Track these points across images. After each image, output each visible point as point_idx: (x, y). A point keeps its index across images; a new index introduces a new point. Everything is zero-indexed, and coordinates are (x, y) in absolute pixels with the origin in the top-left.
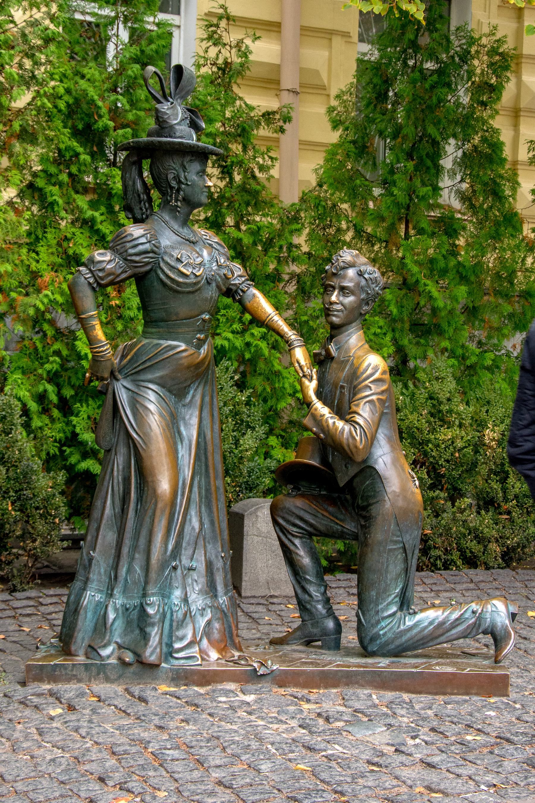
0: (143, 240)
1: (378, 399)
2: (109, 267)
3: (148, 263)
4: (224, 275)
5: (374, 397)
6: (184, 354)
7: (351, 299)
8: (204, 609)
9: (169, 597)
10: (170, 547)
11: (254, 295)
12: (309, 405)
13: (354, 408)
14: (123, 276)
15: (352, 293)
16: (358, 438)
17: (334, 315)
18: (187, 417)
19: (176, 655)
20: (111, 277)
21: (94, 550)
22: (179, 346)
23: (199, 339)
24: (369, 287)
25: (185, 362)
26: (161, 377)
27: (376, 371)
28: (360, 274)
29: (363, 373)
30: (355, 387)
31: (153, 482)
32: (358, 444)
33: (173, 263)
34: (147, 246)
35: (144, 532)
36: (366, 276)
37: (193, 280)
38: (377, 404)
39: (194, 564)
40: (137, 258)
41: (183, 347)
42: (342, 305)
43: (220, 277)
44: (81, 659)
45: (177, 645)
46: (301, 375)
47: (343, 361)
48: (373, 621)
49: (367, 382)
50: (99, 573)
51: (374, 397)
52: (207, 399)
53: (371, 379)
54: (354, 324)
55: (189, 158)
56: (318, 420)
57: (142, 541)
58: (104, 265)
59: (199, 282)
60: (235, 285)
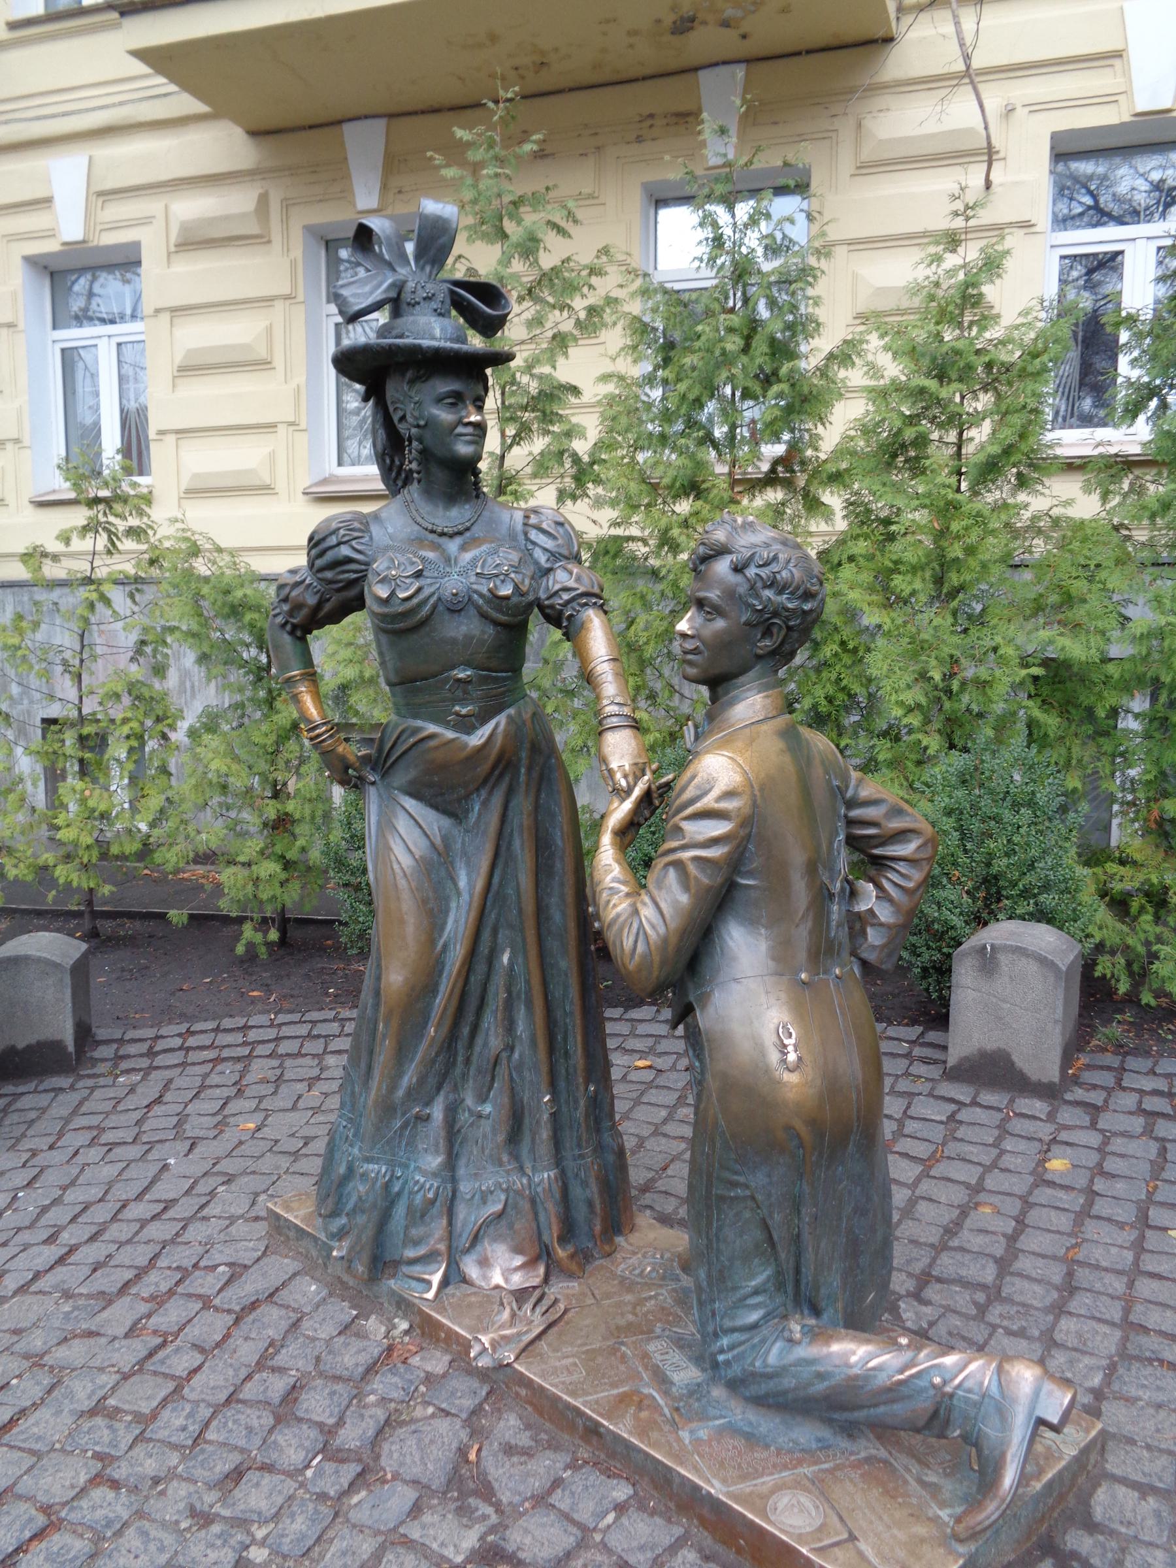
0: (333, 540)
1: (696, 859)
2: (294, 594)
4: (490, 590)
5: (687, 855)
6: (433, 743)
7: (720, 624)
9: (405, 1166)
11: (582, 626)
14: (327, 607)
20: (304, 612)
22: (418, 730)
23: (457, 714)
24: (758, 596)
27: (706, 793)
28: (738, 569)
34: (345, 551)
41: (432, 728)
43: (481, 595)
45: (410, 1253)
54: (742, 679)
60: (552, 607)
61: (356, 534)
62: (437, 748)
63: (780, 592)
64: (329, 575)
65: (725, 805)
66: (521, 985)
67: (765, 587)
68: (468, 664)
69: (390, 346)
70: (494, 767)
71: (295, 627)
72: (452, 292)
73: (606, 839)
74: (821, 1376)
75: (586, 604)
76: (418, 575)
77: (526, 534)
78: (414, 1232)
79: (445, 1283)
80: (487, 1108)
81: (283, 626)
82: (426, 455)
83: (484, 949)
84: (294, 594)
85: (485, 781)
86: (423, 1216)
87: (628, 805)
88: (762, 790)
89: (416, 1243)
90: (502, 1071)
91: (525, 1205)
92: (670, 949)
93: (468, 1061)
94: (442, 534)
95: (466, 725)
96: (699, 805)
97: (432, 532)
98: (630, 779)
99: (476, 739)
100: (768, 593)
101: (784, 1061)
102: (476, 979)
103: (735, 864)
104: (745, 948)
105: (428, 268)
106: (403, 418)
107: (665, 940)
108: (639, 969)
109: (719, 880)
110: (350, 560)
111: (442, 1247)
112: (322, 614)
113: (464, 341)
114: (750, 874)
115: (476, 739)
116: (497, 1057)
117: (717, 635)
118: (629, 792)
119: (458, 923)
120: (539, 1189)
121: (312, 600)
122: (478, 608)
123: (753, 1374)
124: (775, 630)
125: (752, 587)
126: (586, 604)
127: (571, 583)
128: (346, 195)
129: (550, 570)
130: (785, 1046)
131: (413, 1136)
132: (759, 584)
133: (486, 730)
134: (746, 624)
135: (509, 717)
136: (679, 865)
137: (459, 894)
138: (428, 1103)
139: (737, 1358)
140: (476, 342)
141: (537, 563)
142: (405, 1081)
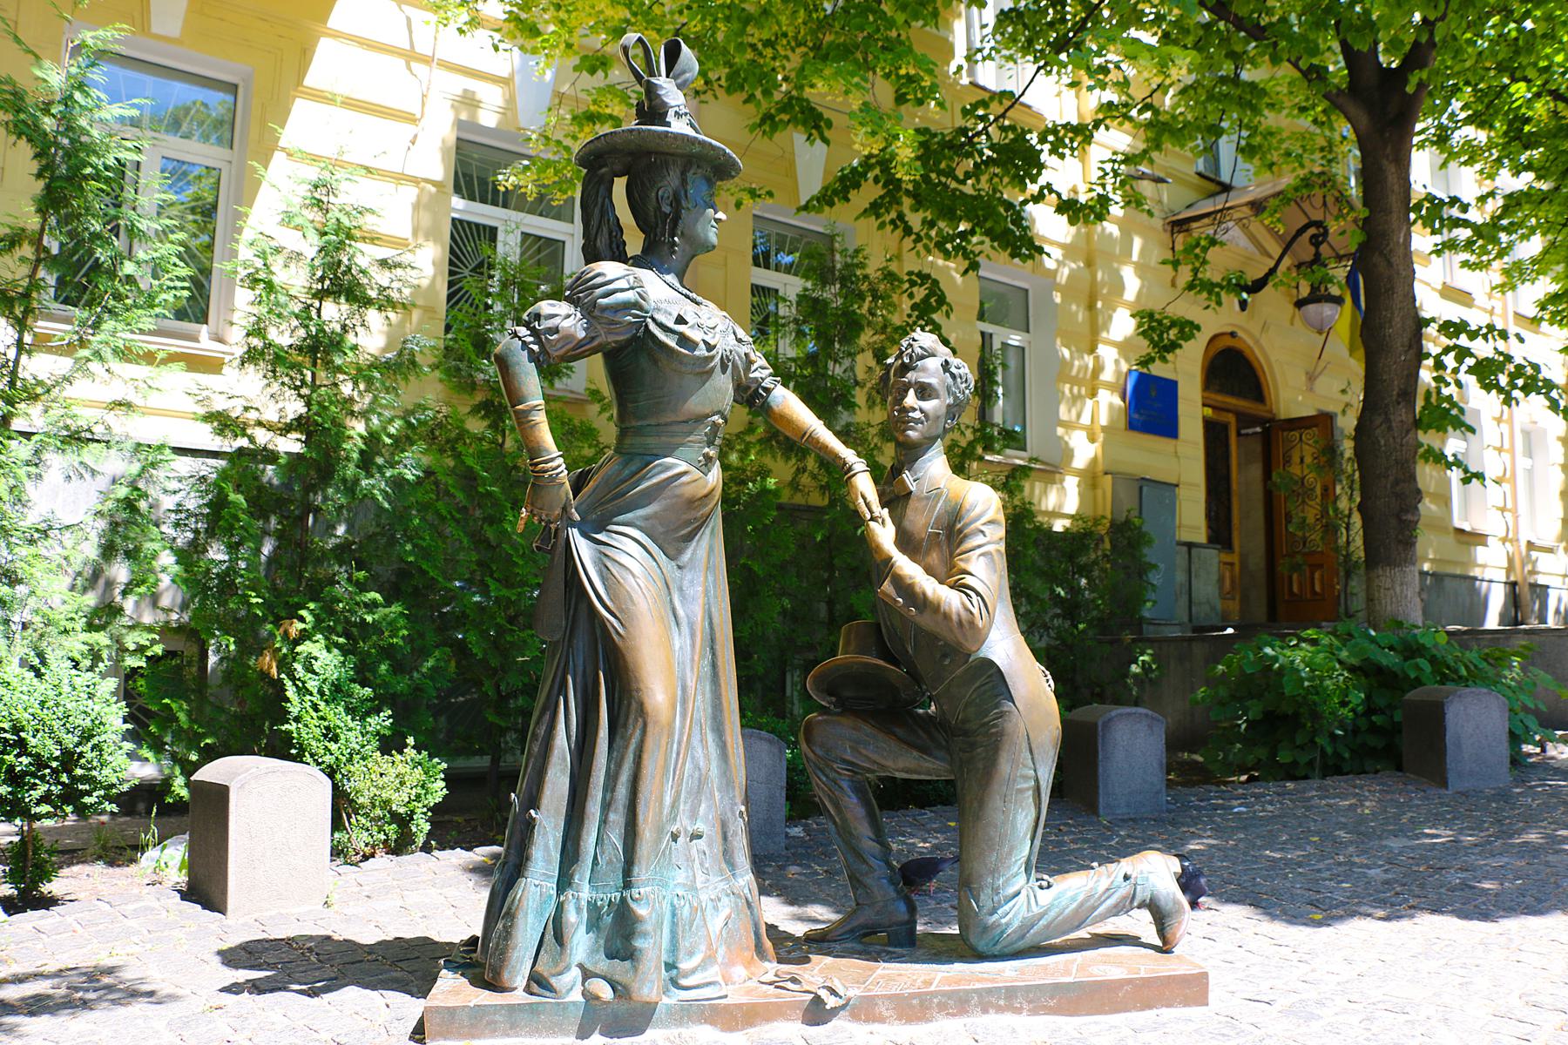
6: (684, 479)
10: (668, 800)
12: (888, 561)
13: (962, 565)
16: (975, 611)
17: (912, 429)
18: (686, 583)
19: (684, 982)
21: (536, 807)
26: (647, 518)
30: (960, 531)
31: (638, 690)
33: (671, 324)
35: (624, 777)
36: (953, 370)
37: (702, 351)
38: (996, 557)
39: (701, 826)
42: (922, 411)
44: (519, 996)
46: (868, 516)
47: (928, 498)
48: (989, 904)
49: (978, 524)
50: (546, 847)
51: (990, 548)
53: (984, 520)
56: (906, 589)
57: (622, 791)
58: (556, 321)
59: (713, 357)
74: (1073, 899)
89: (691, 954)
110: (636, 305)
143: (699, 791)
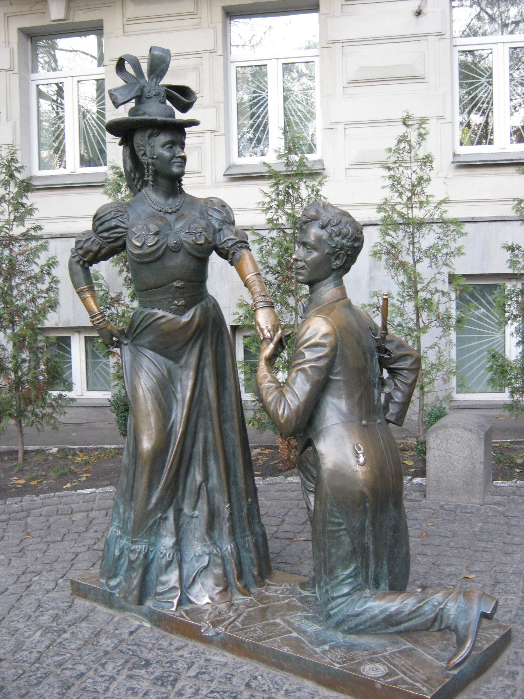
0: (108, 217)
1: (311, 367)
2: (85, 246)
3: (117, 239)
4: (193, 241)
5: (306, 366)
6: (163, 320)
7: (315, 254)
8: (201, 556)
10: (154, 500)
14: (103, 251)
15: (315, 248)
16: (280, 412)
18: (184, 377)
20: (91, 254)
22: (155, 314)
24: (333, 240)
25: (165, 327)
26: (150, 342)
27: (315, 335)
29: (301, 338)
32: (280, 417)
40: (105, 234)
42: (305, 262)
46: (262, 338)
51: (306, 366)
52: (209, 359)
54: (326, 281)
55: (148, 132)
60: (223, 249)
61: (120, 214)
62: (164, 323)
63: (343, 238)
64: (105, 234)
65: (322, 341)
66: (210, 447)
67: (337, 236)
68: (181, 280)
69: (141, 120)
70: (194, 333)
71: (85, 262)
72: (167, 91)
73: (262, 364)
74: (382, 612)
75: (241, 247)
76: (157, 234)
77: (207, 212)
78: (163, 578)
79: (180, 603)
80: (196, 513)
81: (78, 262)
82: (156, 173)
83: (191, 429)
84: (85, 246)
85: (191, 338)
86: (166, 569)
87: (272, 346)
88: (340, 333)
89: (163, 584)
90: (204, 493)
91: (219, 561)
92: (301, 411)
93: (184, 489)
94: (166, 212)
95: (182, 311)
96: (313, 341)
97: (161, 211)
98: (272, 333)
99: (185, 318)
100: (337, 239)
101: (358, 461)
102: (189, 442)
103: (329, 369)
104: (335, 410)
105: (155, 80)
106: (144, 154)
107: (298, 407)
108: (287, 421)
109: (323, 377)
110: (117, 227)
111: (177, 585)
112: (100, 255)
113: (173, 116)
114: (337, 374)
115: (185, 318)
116: (201, 485)
117: (314, 260)
118: (271, 339)
119: (179, 415)
120: (226, 553)
121: (96, 248)
122: (186, 249)
123: (349, 616)
124: (341, 256)
125: (330, 236)
126: (241, 247)
127: (232, 237)
128: (45, 12)
129: (220, 230)
130: (358, 454)
131: (158, 530)
132: (334, 235)
133: (191, 313)
134: (328, 254)
135: (202, 306)
136: (303, 370)
137: (177, 400)
138: (165, 511)
139: (339, 611)
140: (180, 116)
141: (213, 226)
142: (154, 500)
143: (199, 494)
